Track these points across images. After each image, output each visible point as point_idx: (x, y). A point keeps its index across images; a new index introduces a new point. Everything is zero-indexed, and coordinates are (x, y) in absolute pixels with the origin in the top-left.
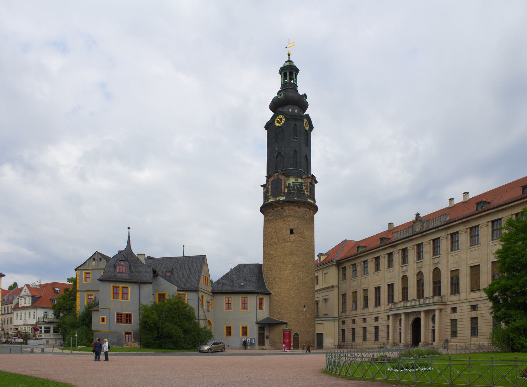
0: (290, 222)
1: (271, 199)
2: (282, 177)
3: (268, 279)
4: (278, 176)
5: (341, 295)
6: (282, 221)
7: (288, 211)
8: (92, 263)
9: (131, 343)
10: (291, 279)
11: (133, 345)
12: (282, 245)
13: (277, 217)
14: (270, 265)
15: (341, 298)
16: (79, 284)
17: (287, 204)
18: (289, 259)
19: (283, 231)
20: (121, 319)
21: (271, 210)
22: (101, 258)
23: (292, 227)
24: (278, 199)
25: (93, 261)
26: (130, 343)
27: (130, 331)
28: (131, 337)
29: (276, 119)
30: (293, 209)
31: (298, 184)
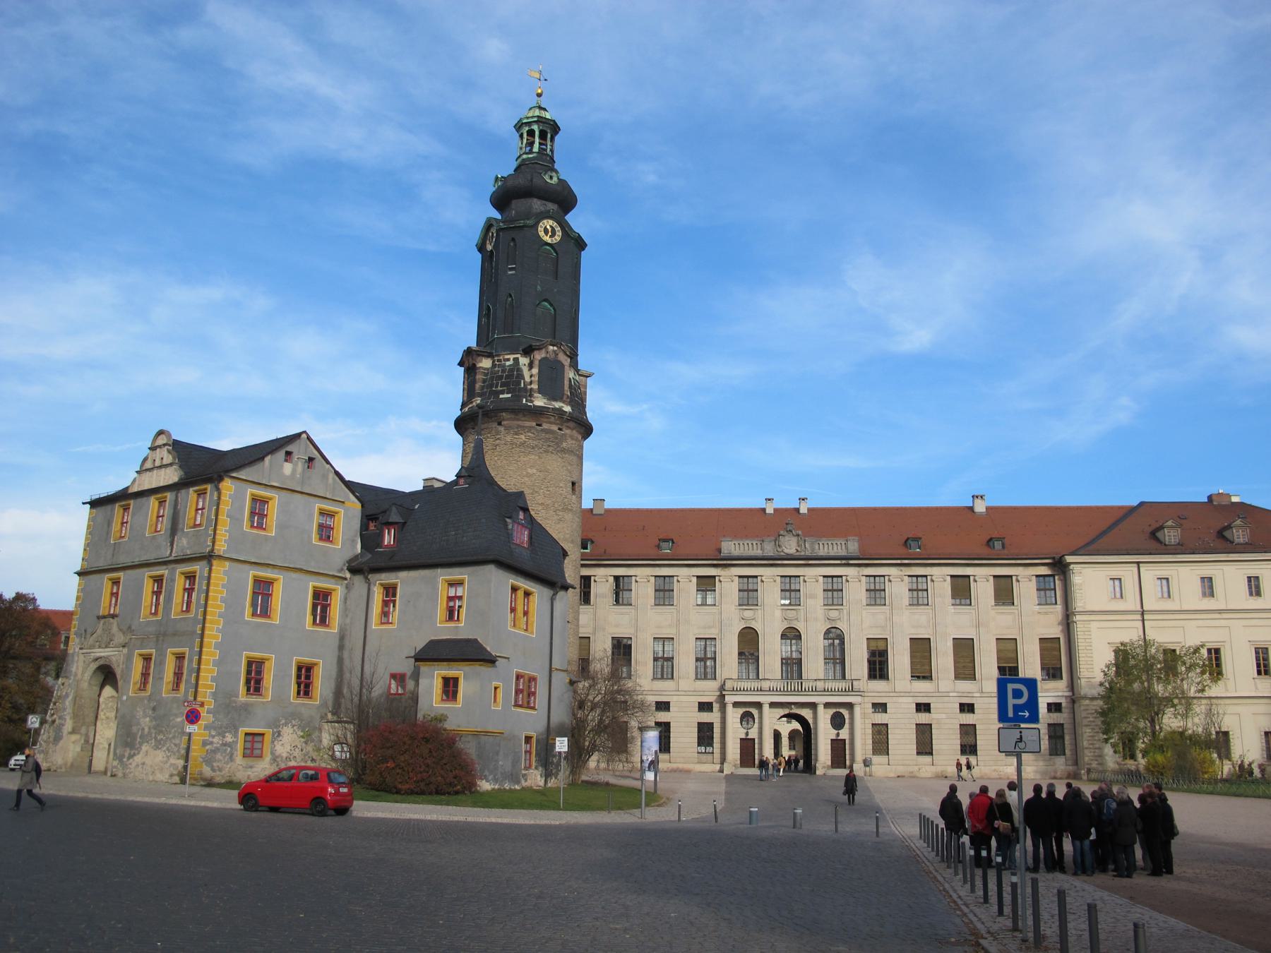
2: (566, 360)
4: (557, 354)
6: (560, 459)
8: (282, 466)
12: (559, 515)
13: (549, 446)
16: (226, 531)
17: (572, 424)
19: (561, 481)
21: (534, 424)
24: (557, 405)
25: (286, 461)
29: (541, 224)
30: (577, 440)
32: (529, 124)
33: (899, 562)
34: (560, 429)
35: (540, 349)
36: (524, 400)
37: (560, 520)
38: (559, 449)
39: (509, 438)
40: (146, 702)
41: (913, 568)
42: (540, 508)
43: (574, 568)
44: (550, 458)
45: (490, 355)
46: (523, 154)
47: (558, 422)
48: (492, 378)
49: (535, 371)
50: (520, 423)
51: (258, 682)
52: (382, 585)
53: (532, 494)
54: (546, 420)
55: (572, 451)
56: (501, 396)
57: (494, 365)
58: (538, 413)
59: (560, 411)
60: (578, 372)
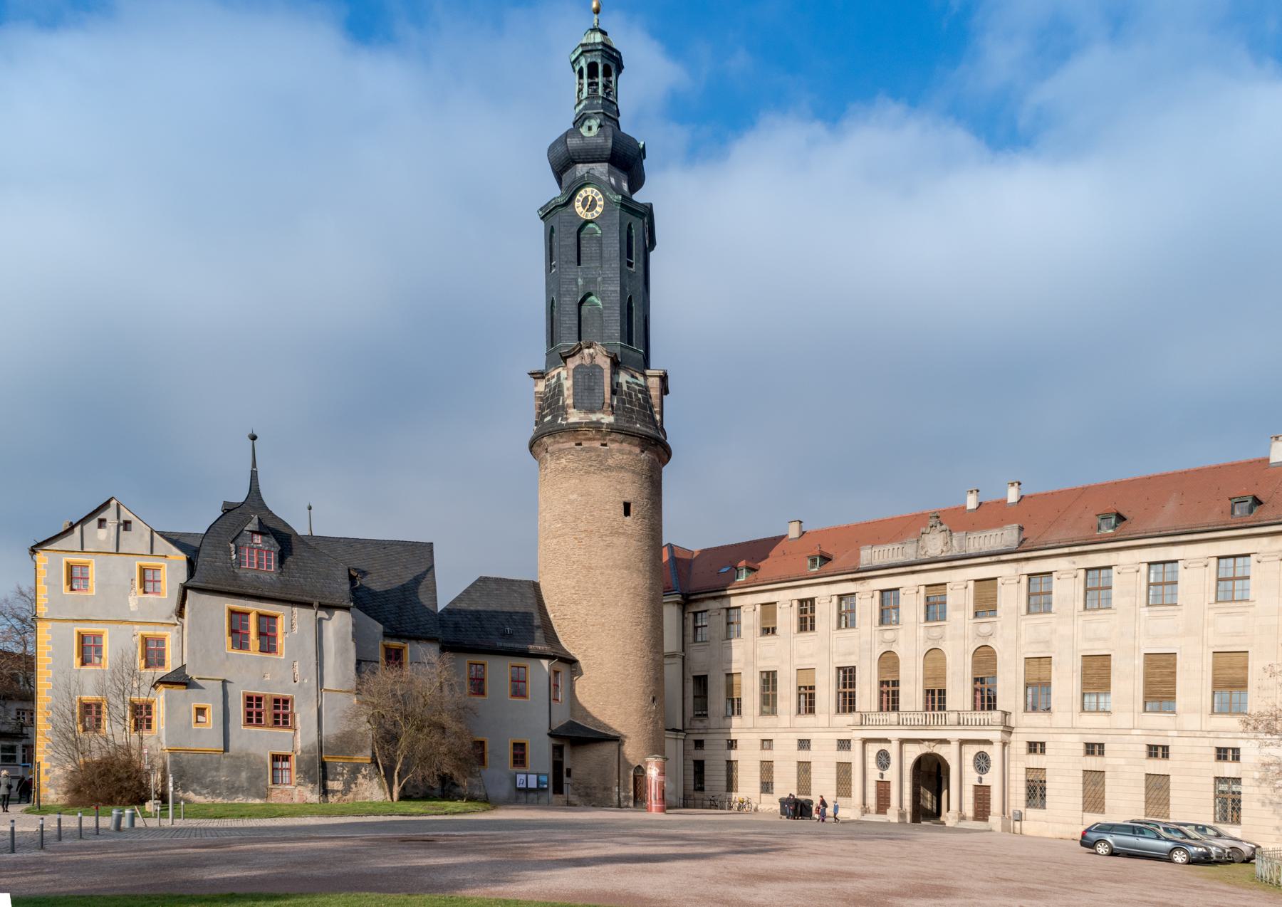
0: (624, 483)
1: (574, 417)
3: (566, 623)
5: (692, 678)
6: (604, 479)
7: (618, 454)
9: (291, 787)
10: (627, 630)
11: (296, 792)
13: (591, 466)
15: (690, 685)
18: (623, 578)
20: (259, 714)
21: (573, 444)
23: (627, 499)
26: (288, 787)
27: (288, 752)
28: (290, 769)
31: (639, 390)
33: (1066, 550)
34: (603, 445)
36: (560, 419)
37: (608, 546)
38: (602, 467)
41: (1091, 556)
42: (584, 535)
43: (632, 596)
44: (592, 479)
47: (598, 437)
50: (561, 446)
53: (574, 522)
54: (583, 437)
55: (623, 468)
58: (573, 429)
59: (597, 426)
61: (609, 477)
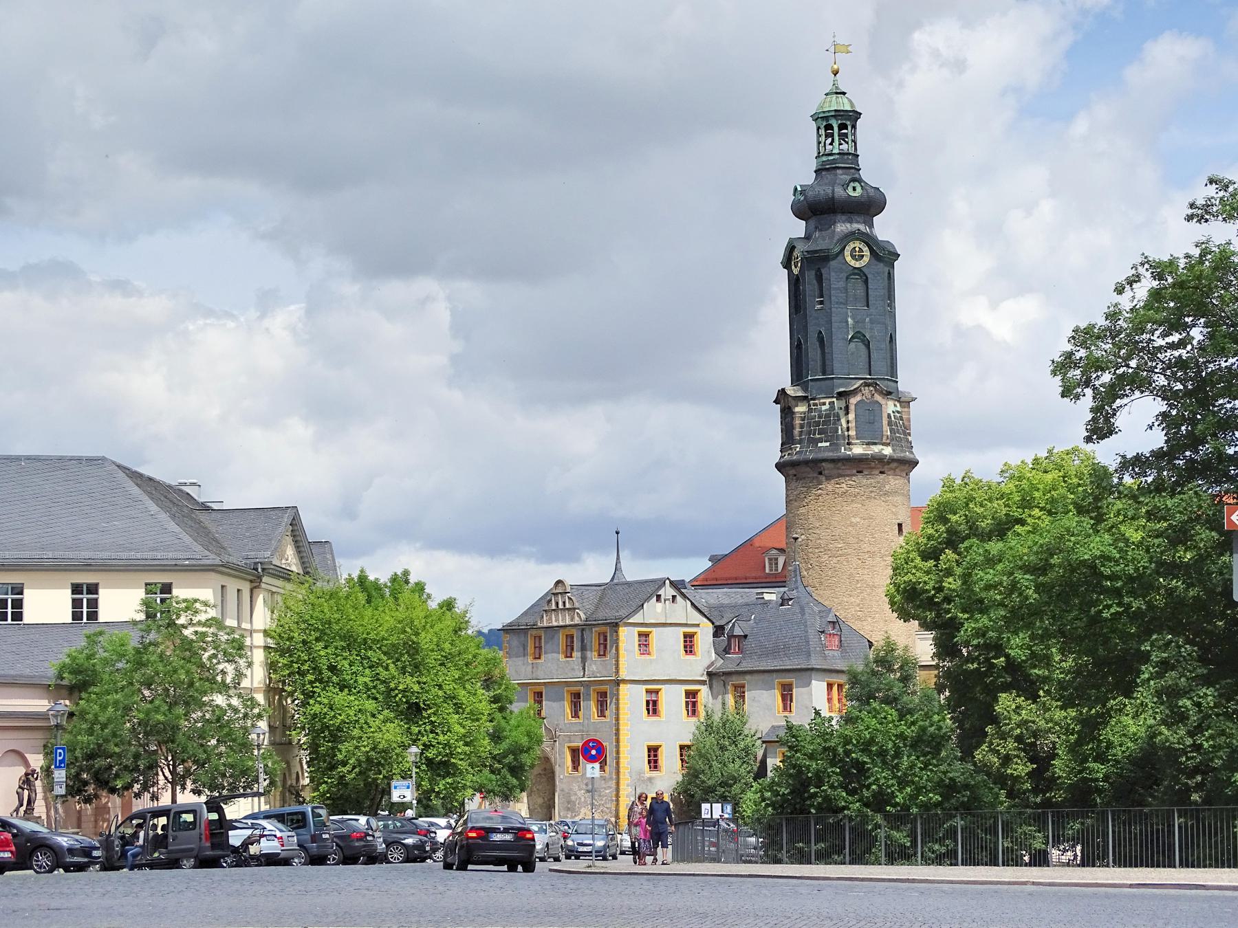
13: (871, 492)
14: (859, 605)
17: (894, 465)
22: (675, 594)
24: (876, 449)
32: (826, 118)
35: (854, 392)
39: (830, 487)
40: (580, 780)
45: (805, 398)
46: (823, 155)
48: (809, 425)
49: (851, 416)
50: (840, 471)
51: (656, 761)
52: (733, 684)
56: (820, 445)
57: (810, 410)
60: (898, 401)
61: (886, 502)
